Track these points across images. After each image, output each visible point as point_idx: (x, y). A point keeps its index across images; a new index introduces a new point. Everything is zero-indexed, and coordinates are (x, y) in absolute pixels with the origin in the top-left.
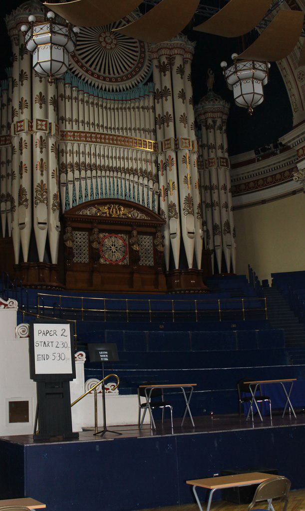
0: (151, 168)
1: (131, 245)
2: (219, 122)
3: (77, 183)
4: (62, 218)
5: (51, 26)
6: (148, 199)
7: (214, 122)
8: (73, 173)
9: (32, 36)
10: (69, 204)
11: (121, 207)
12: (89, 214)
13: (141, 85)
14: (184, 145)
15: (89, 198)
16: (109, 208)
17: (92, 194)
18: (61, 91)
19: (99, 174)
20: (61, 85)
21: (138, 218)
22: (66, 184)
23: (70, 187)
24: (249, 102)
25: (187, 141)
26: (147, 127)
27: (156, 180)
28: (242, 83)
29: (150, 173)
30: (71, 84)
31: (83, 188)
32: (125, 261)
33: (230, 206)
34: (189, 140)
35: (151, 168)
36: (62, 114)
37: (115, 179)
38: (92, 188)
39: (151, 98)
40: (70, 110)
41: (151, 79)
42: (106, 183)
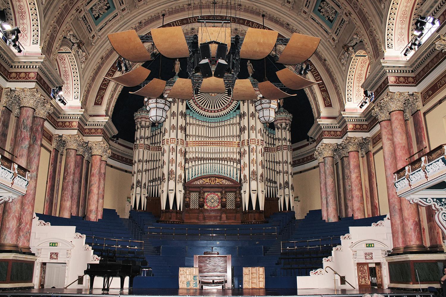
0: (236, 156)
1: (222, 198)
2: (284, 125)
3: (194, 168)
4: (185, 188)
5: (156, 100)
7: (281, 125)
8: (192, 163)
9: (148, 104)
10: (189, 179)
11: (216, 178)
12: (199, 183)
13: (231, 112)
14: (252, 142)
15: (199, 175)
16: (210, 180)
18: (188, 121)
19: (212, 162)
20: (188, 118)
21: (227, 184)
23: (190, 170)
24: (267, 121)
25: (254, 140)
26: (235, 134)
27: (239, 162)
28: (264, 110)
29: (235, 159)
30: (193, 117)
31: (196, 170)
32: (219, 207)
33: (290, 172)
34: (255, 139)
35: (236, 156)
36: (188, 133)
39: (238, 118)
40: (191, 130)
41: (239, 108)
42: (208, 167)
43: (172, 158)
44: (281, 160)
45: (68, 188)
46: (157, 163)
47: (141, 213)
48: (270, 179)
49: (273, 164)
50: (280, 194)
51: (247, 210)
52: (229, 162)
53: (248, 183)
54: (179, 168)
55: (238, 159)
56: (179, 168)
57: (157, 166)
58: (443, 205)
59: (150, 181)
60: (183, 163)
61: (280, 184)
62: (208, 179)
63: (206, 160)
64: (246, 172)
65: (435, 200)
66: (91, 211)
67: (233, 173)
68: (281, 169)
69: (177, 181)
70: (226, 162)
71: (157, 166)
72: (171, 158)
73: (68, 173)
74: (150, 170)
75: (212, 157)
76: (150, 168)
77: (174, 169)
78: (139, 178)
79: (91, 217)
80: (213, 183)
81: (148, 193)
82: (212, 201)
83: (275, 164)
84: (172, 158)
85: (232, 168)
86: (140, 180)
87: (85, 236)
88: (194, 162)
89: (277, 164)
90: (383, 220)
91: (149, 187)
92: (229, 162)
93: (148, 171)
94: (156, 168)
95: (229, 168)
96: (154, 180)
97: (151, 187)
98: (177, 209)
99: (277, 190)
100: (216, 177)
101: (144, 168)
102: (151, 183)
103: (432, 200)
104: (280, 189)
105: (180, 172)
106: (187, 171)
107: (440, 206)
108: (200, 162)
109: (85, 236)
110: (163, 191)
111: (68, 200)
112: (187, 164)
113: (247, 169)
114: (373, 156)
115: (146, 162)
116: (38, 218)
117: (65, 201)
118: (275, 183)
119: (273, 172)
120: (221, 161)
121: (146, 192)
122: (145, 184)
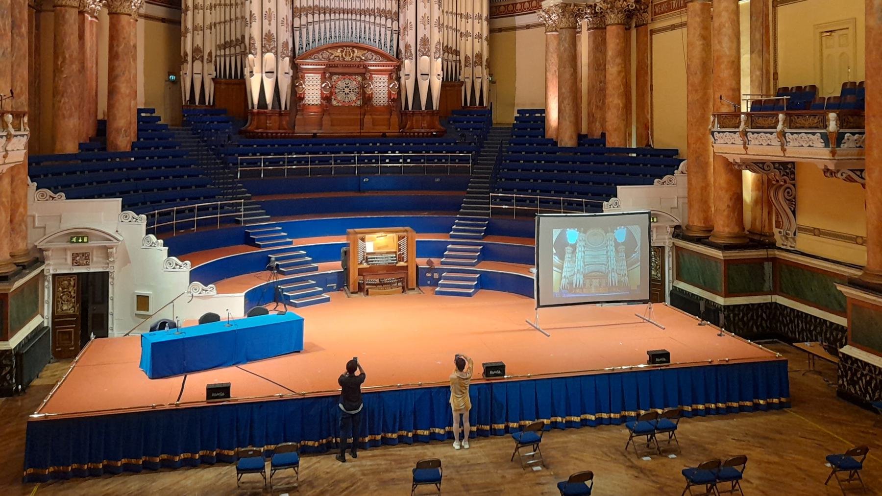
6: (386, 39)
16: (342, 52)
17: (325, 38)
22: (300, 28)
23: (304, 31)
29: (390, 12)
37: (350, 22)
38: (325, 32)
43: (270, 9)
44: (470, 13)
45: (69, 91)
46: (233, 10)
47: (206, 112)
48: (447, 46)
49: (454, 18)
50: (465, 74)
51: (410, 108)
52: (378, 18)
53: (414, 60)
54: (282, 29)
55: (394, 11)
56: (282, 29)
57: (233, 17)
58: (788, 173)
59: (219, 47)
60: (290, 19)
61: (466, 57)
62: (339, 51)
63: (335, 13)
64: (410, 38)
65: (777, 165)
66: (118, 131)
67: (386, 39)
68: (470, 30)
69: (279, 55)
70: (372, 17)
71: (233, 17)
72: (265, 9)
73: (64, 58)
74: (220, 23)
75: (346, 7)
76: (218, 21)
77: (274, 31)
78: (199, 42)
79: (119, 143)
80: (348, 58)
81: (216, 70)
82: (347, 90)
83: (459, 18)
84: (270, 9)
85: (383, 30)
86: (201, 45)
87: (144, 216)
88: (310, 16)
89: (461, 18)
90: (673, 174)
91: (218, 59)
92: (378, 18)
93: (215, 24)
94: (231, 20)
95: (377, 29)
96: (226, 45)
97: (223, 59)
98: (280, 108)
99: (460, 67)
100: (354, 47)
101: (208, 22)
102: (223, 51)
103: (772, 165)
104: (466, 66)
105: (284, 36)
106: (297, 34)
107: (784, 175)
108: (322, 15)
109: (144, 216)
110: (251, 72)
111: (71, 115)
112: (297, 20)
113: (412, 33)
114: (651, 35)
115: (211, 9)
116: (36, 184)
117: (64, 117)
118: (457, 53)
119: (454, 34)
120: (363, 16)
121: (213, 68)
122: (210, 54)
